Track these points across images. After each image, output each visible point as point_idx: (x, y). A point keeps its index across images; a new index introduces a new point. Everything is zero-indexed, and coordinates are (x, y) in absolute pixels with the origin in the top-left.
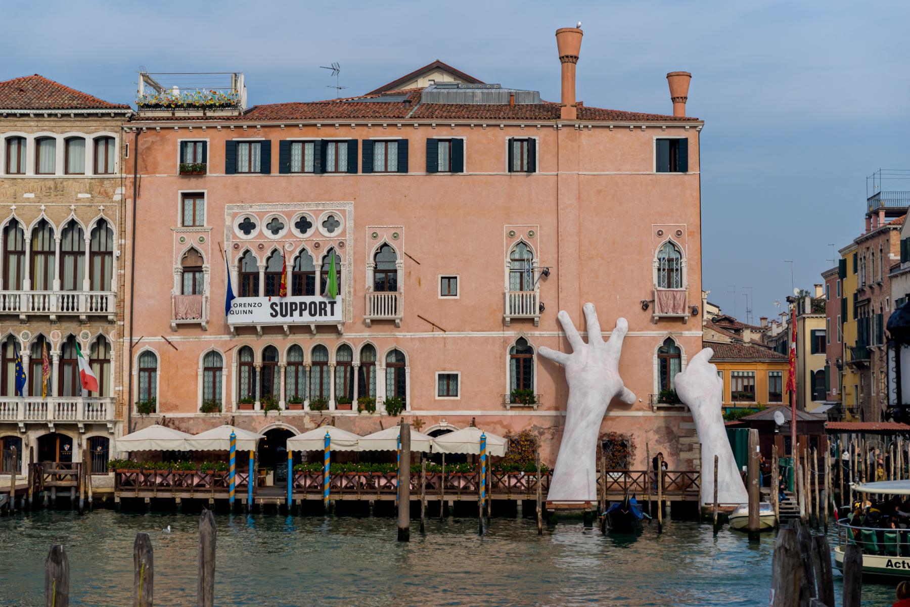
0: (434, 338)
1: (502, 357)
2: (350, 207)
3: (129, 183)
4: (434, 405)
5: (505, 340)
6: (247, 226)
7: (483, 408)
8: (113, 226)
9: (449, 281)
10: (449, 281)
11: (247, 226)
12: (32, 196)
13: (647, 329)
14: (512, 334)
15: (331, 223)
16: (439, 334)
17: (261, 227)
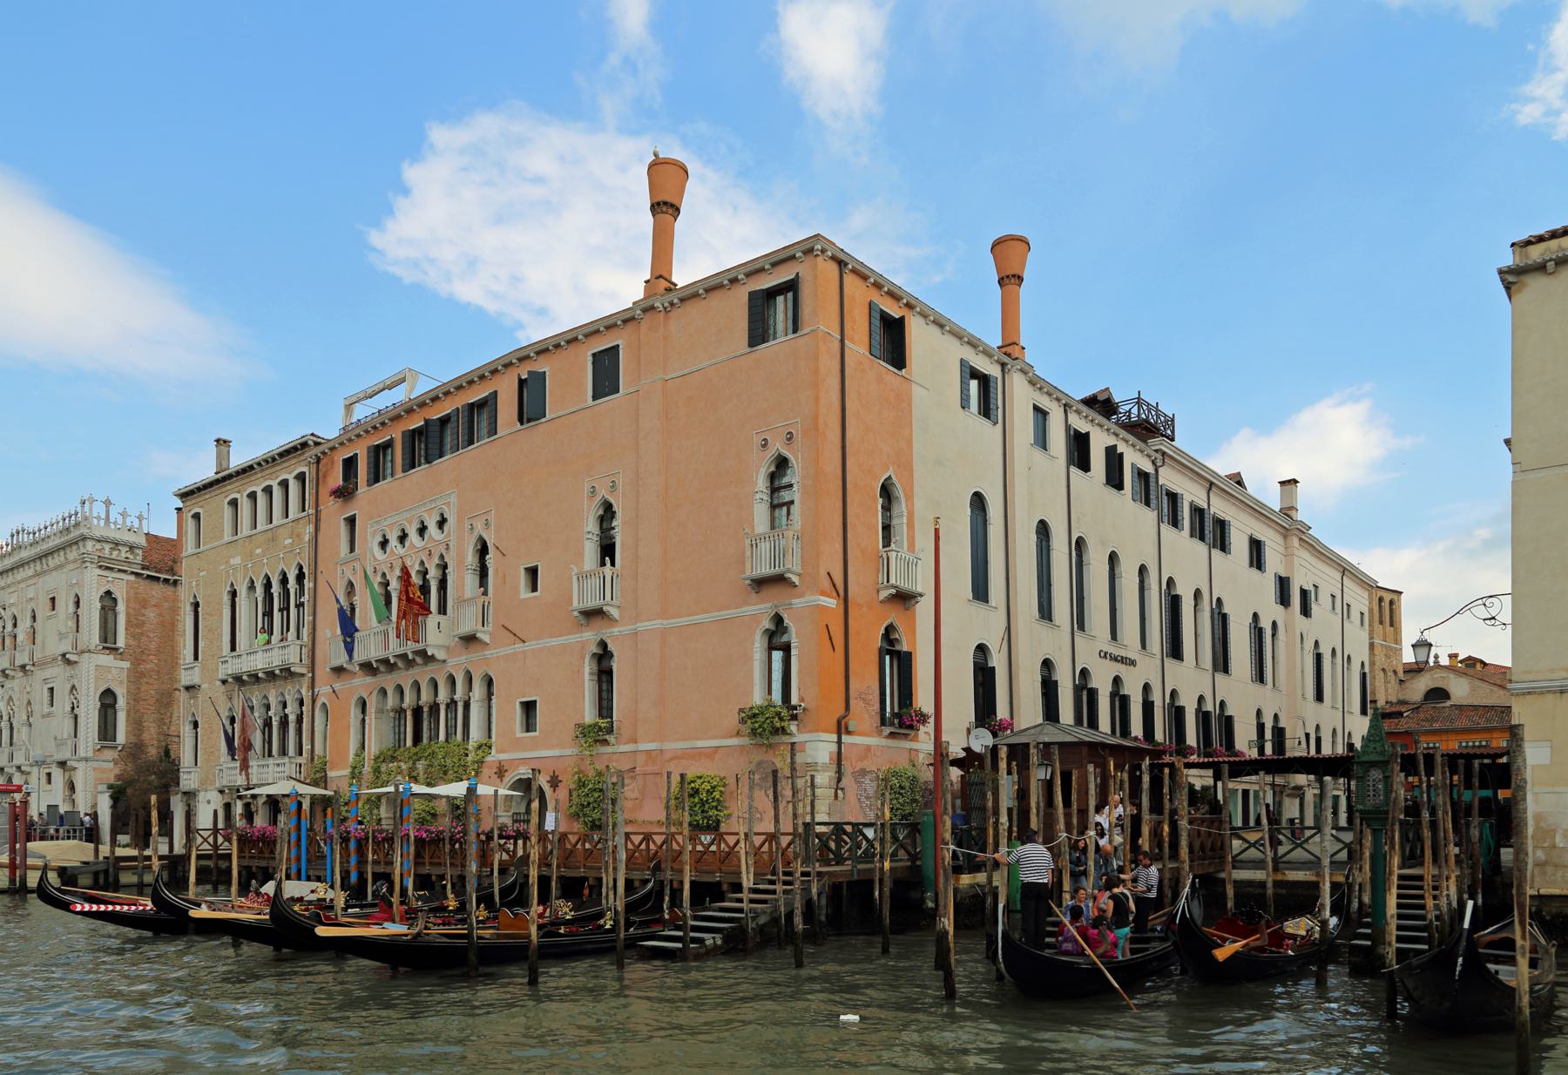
0: (515, 654)
1: (580, 671)
2: (453, 499)
3: (313, 518)
4: (518, 744)
5: (583, 644)
6: (384, 544)
7: (562, 746)
8: (305, 570)
9: (533, 572)
10: (533, 572)
11: (384, 544)
12: (259, 551)
13: (746, 603)
14: (589, 637)
15: (442, 523)
16: (519, 645)
17: (393, 542)
